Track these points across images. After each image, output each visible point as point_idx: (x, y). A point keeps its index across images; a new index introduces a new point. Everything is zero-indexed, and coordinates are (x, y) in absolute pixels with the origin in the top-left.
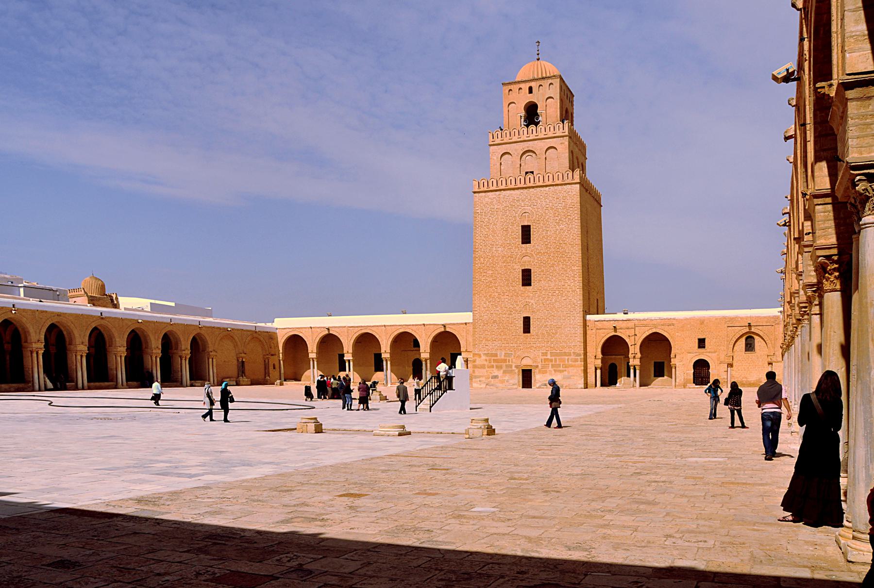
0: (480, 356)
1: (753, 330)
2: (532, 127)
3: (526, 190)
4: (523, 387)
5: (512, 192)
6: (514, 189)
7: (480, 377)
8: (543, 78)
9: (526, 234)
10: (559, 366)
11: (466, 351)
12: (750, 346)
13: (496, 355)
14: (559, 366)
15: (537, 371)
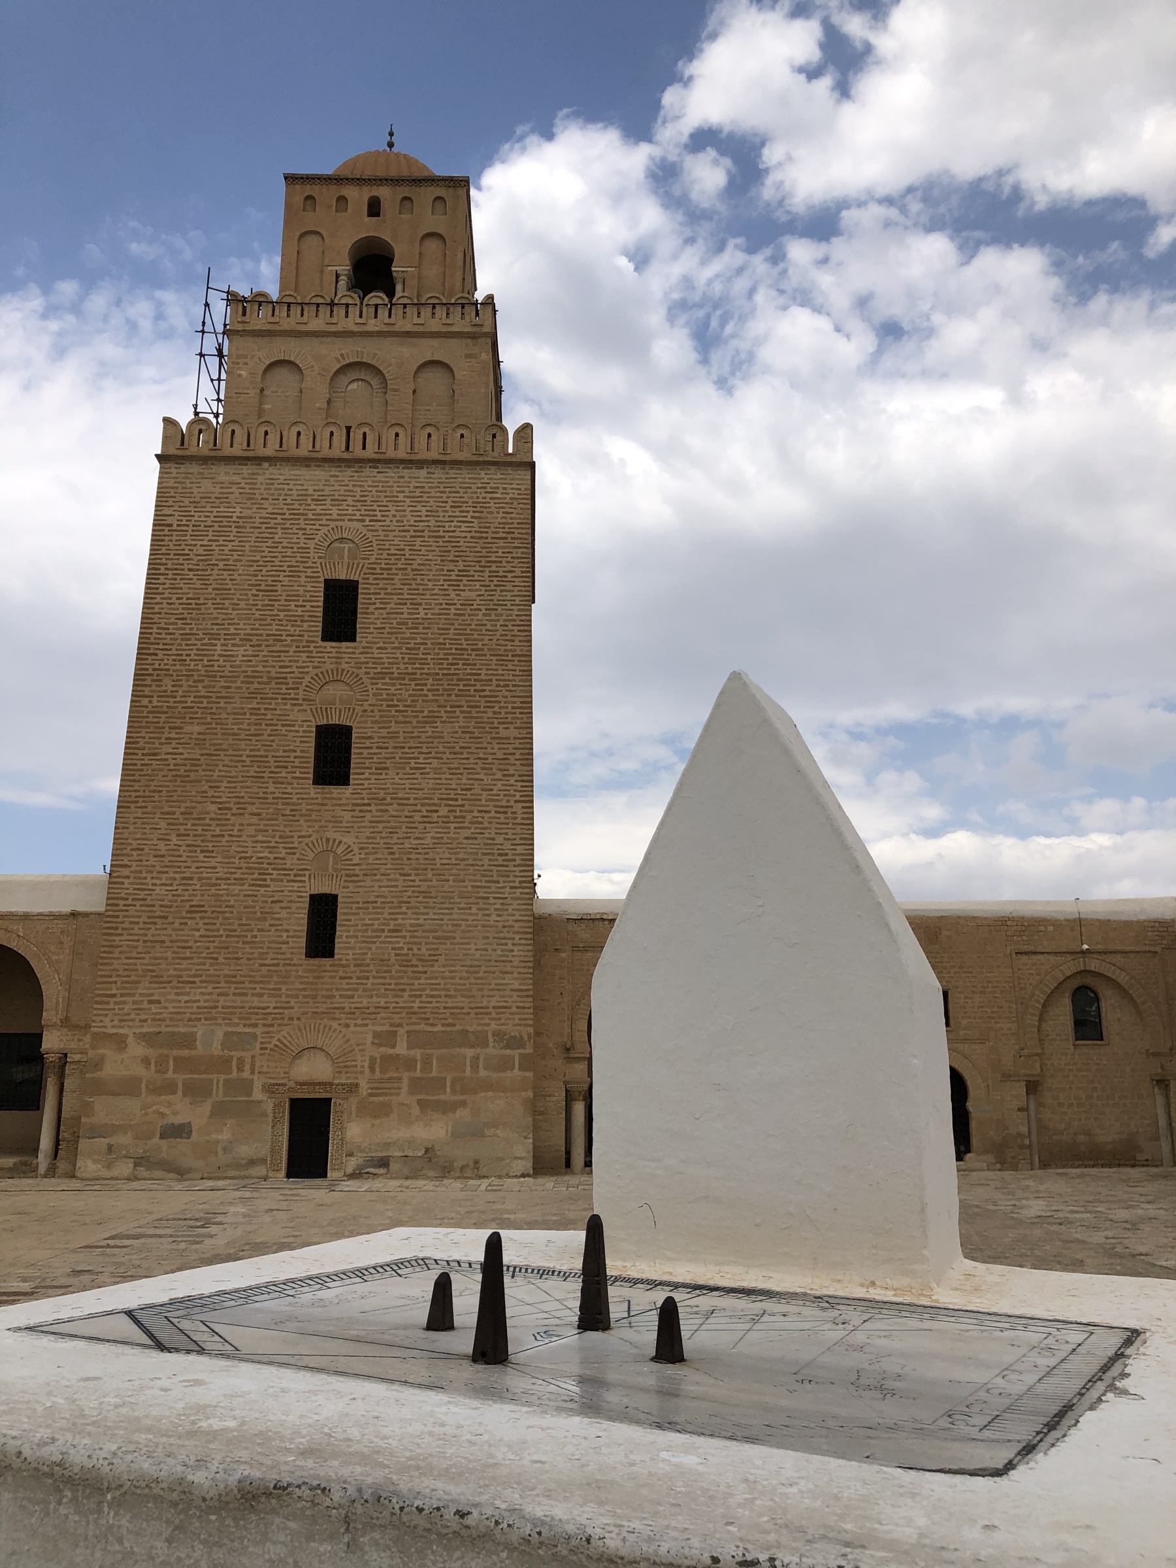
0: (120, 1043)
1: (1094, 965)
2: (377, 297)
3: (346, 474)
4: (289, 1175)
5: (301, 472)
6: (305, 462)
7: (114, 1129)
8: (417, 182)
9: (340, 611)
10: (440, 1083)
11: (66, 1023)
12: (1088, 1026)
13: (188, 1041)
14: (440, 1083)
15: (353, 1104)
